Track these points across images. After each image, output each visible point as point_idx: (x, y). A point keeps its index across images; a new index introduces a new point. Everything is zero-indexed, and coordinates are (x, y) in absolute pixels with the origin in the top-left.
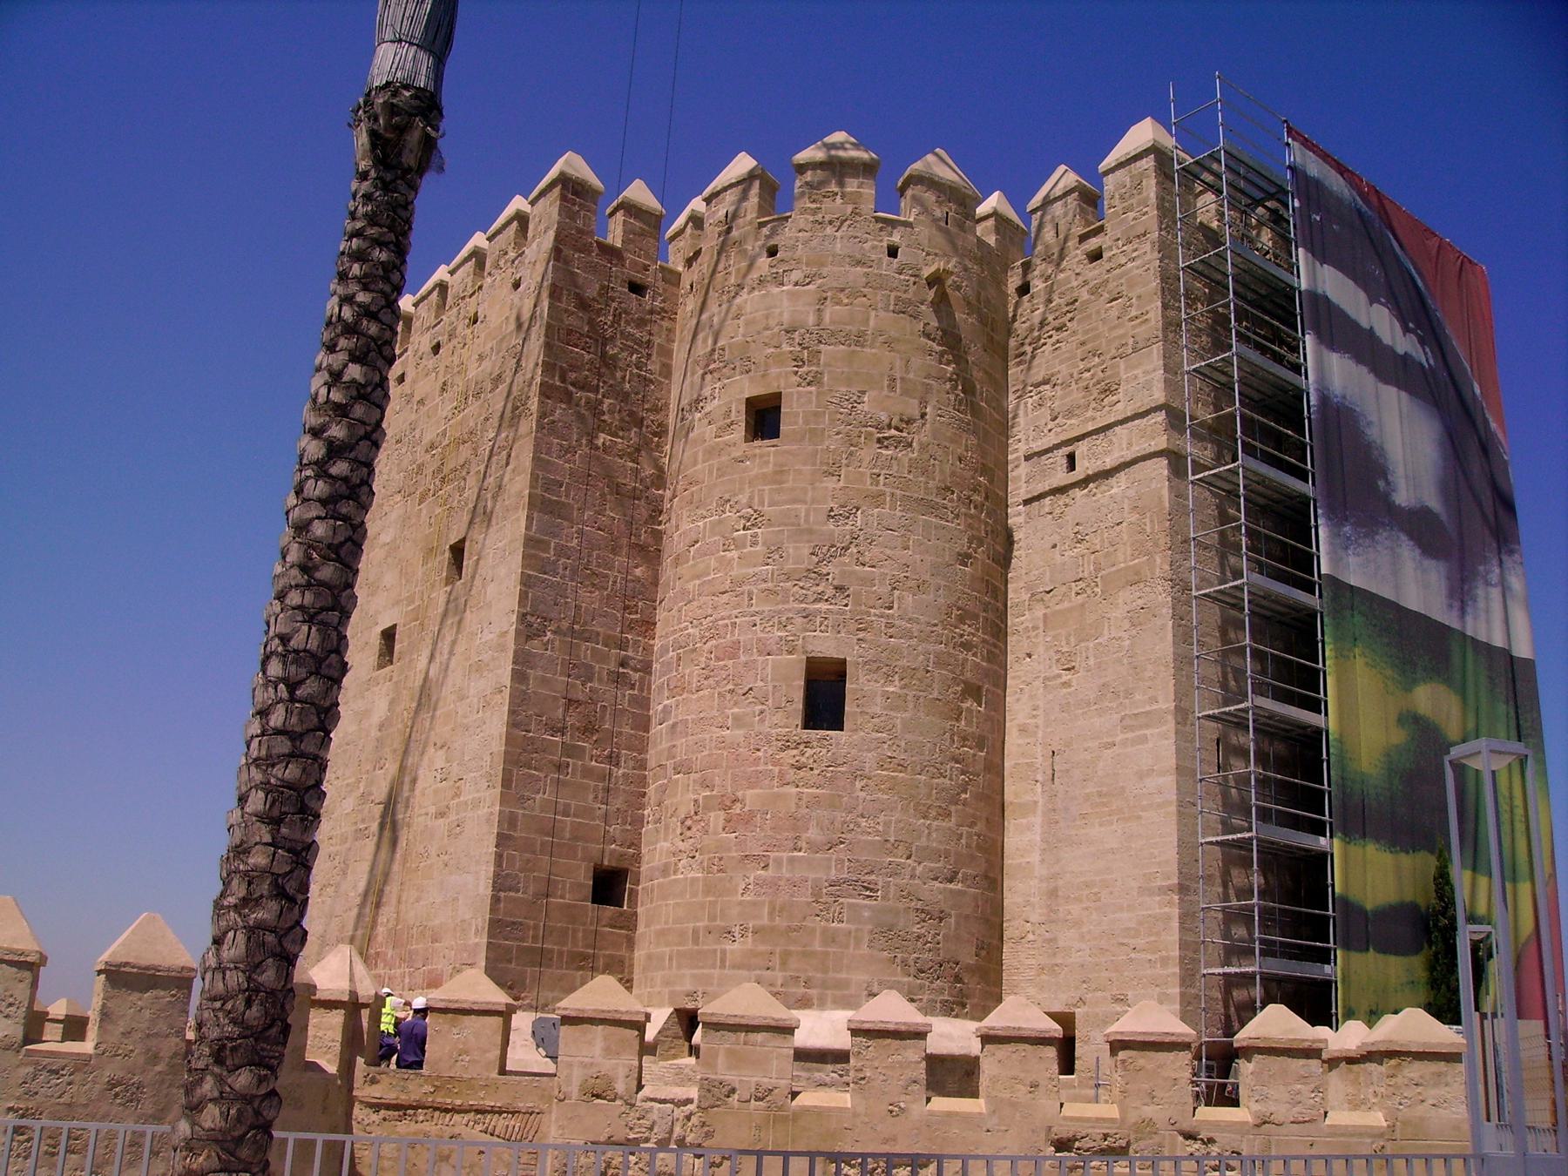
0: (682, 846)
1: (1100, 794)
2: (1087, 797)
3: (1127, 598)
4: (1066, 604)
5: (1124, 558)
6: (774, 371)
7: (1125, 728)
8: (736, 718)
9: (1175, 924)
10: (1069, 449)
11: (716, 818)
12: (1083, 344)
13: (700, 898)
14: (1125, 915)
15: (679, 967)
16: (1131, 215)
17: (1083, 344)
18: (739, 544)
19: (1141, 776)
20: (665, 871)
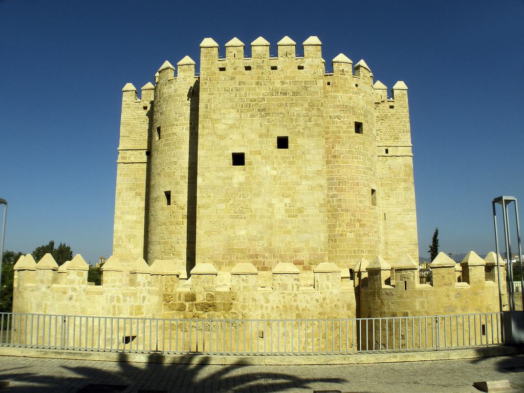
0: (347, 230)
1: (398, 224)
2: (395, 224)
3: (403, 185)
4: (386, 182)
5: (402, 176)
6: (361, 117)
7: (404, 211)
8: (360, 201)
9: (418, 251)
10: (386, 148)
11: (357, 224)
12: (389, 126)
13: (355, 243)
14: (405, 249)
15: (350, 259)
16: (402, 102)
17: (389, 126)
18: (356, 158)
19: (408, 221)
20: (342, 235)
